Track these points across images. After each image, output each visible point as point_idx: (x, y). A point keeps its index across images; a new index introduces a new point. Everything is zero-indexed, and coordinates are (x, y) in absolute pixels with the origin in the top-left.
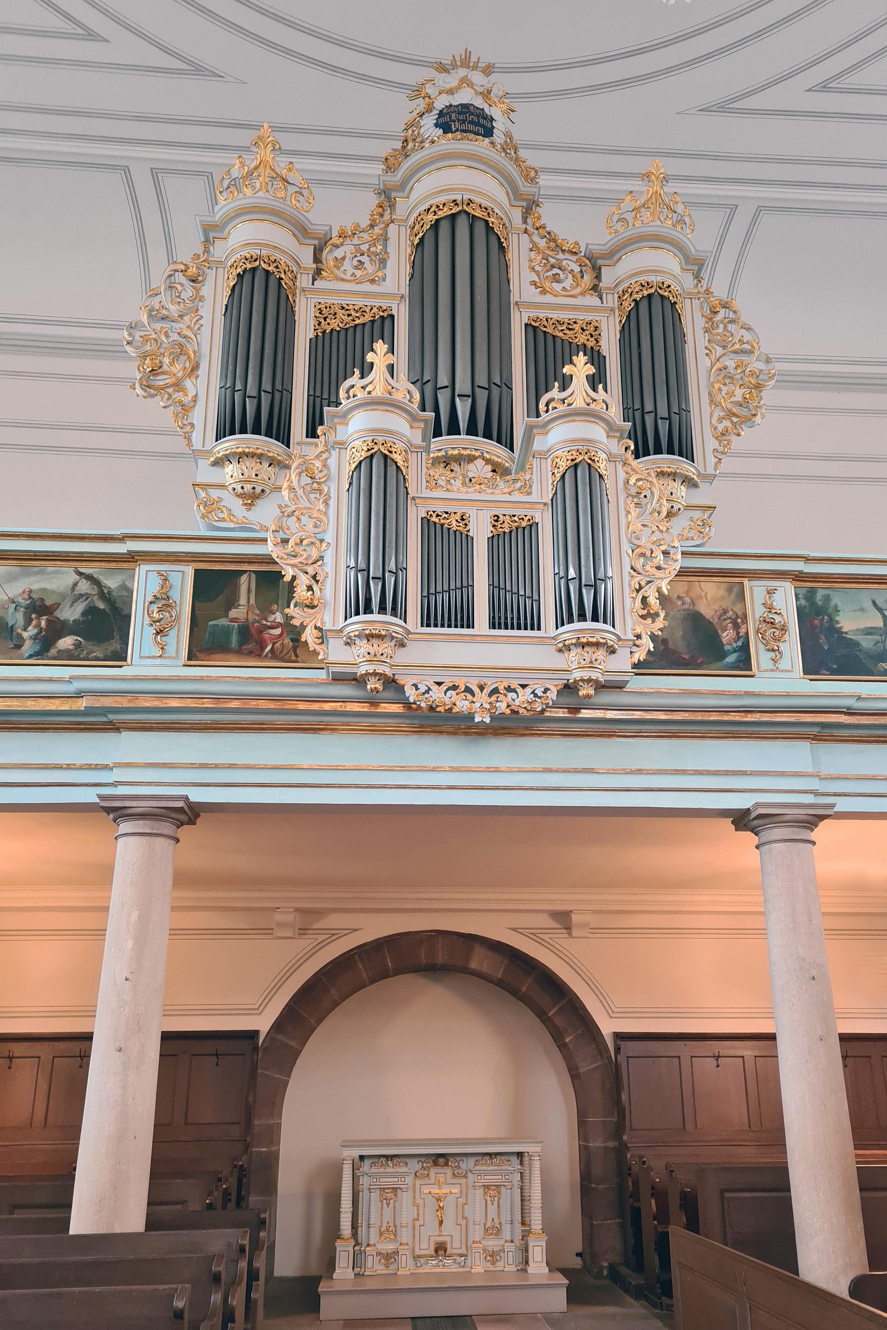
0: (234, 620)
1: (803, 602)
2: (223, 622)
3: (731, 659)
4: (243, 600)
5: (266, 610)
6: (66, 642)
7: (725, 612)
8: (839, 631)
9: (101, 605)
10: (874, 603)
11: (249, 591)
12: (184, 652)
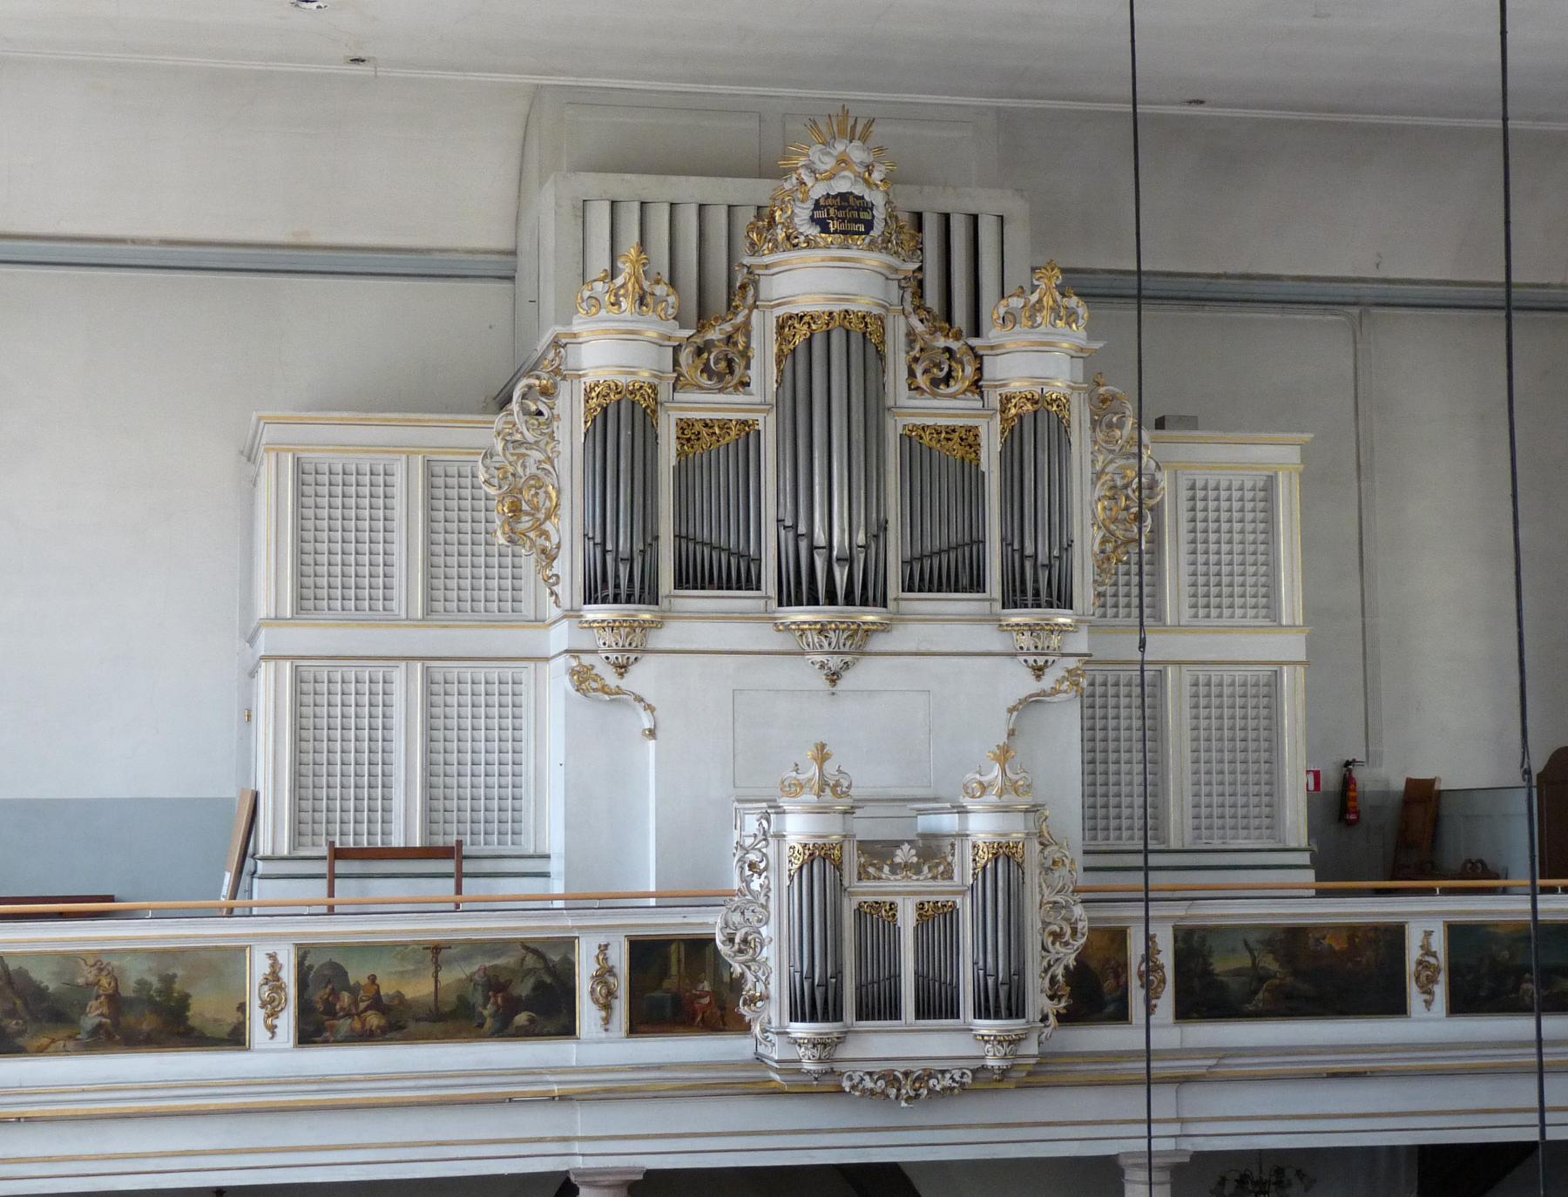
0: (668, 990)
1: (1181, 945)
2: (657, 994)
3: (1110, 1009)
4: (674, 970)
5: (696, 981)
6: (522, 1018)
7: (1108, 960)
8: (1210, 973)
9: (548, 980)
10: (1246, 944)
11: (679, 961)
12: (625, 1025)
